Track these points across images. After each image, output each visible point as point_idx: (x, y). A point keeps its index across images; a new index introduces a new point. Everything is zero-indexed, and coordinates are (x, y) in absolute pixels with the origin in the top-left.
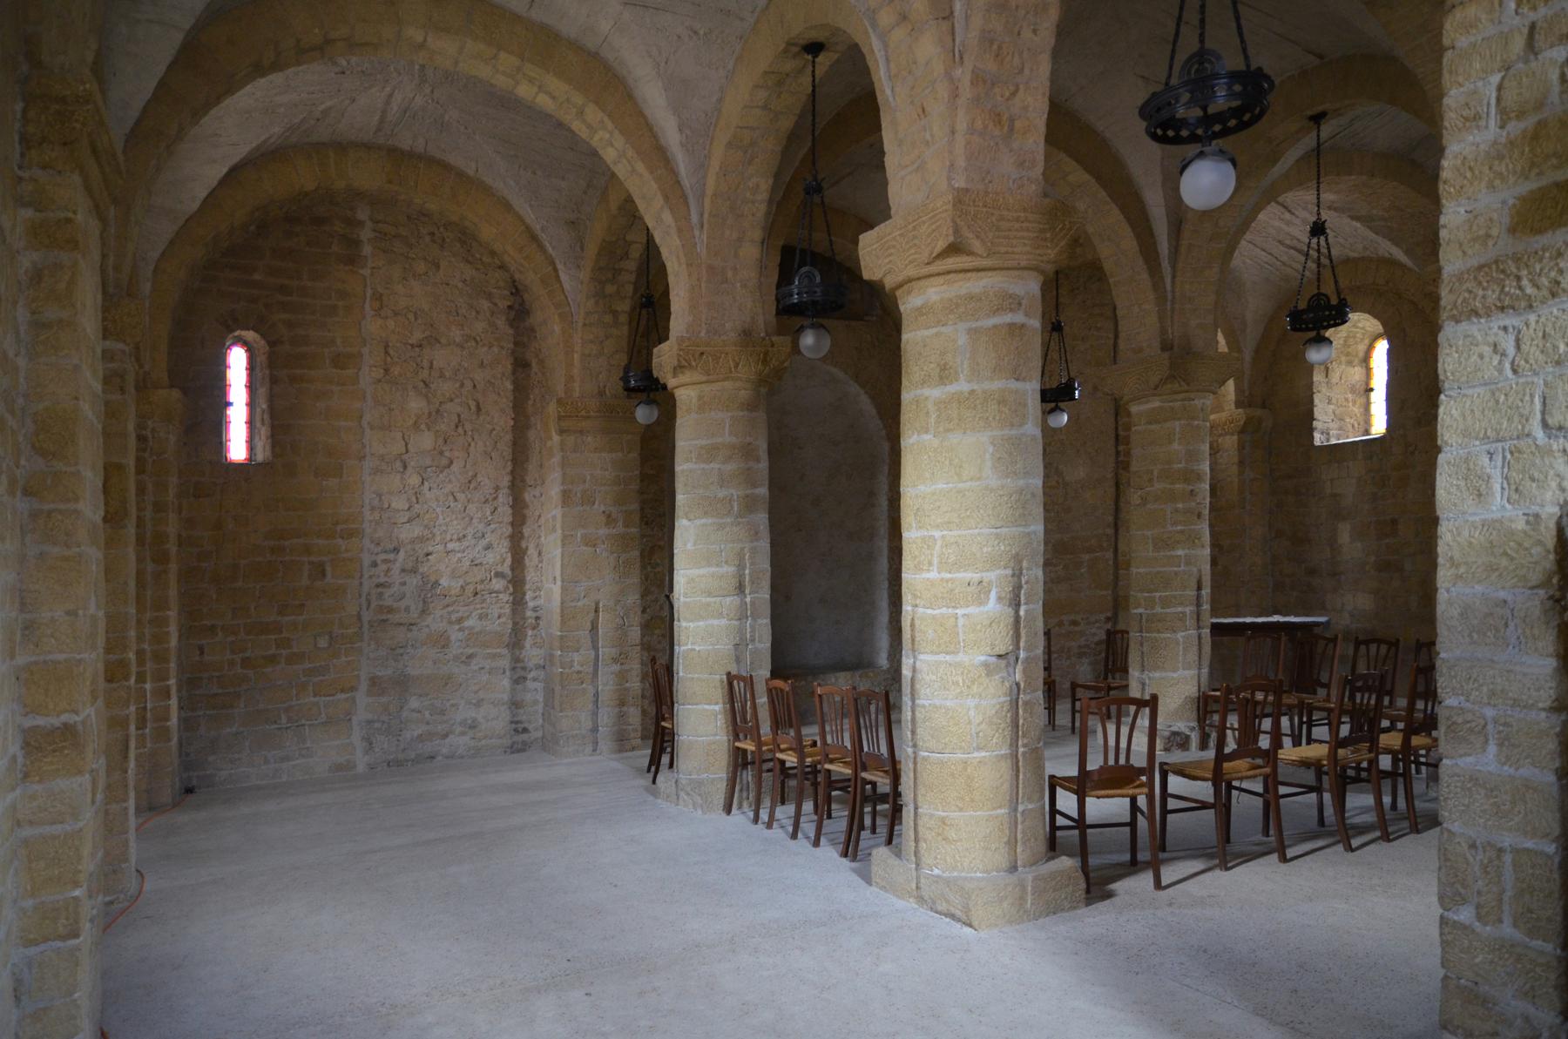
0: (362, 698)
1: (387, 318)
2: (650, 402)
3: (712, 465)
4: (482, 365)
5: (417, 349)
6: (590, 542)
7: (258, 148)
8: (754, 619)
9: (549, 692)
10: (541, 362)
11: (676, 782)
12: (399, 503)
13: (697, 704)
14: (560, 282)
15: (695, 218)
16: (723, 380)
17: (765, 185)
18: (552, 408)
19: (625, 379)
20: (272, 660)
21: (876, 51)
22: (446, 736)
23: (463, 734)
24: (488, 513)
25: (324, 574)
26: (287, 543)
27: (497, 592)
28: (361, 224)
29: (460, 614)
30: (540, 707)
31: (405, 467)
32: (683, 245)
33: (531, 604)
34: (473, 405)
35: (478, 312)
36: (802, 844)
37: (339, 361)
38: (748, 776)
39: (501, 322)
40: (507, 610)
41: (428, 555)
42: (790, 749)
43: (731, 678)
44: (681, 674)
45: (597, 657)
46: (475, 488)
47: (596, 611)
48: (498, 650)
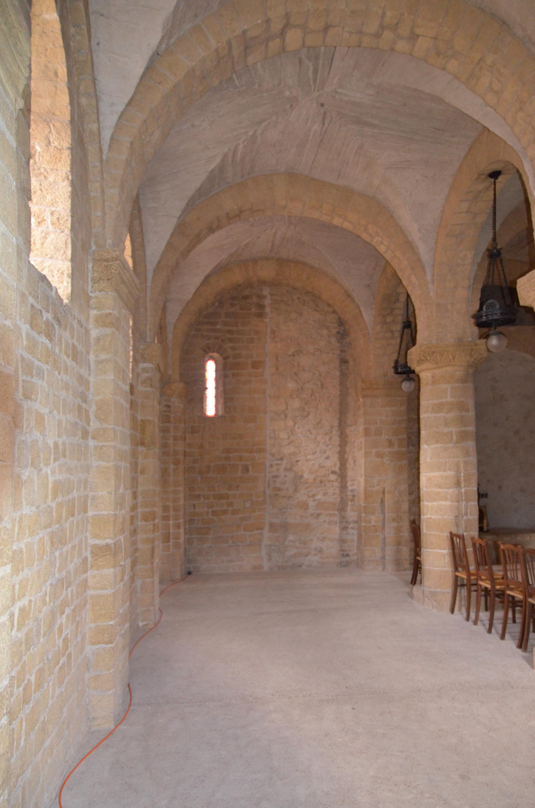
0: (266, 534)
2: (410, 379)
5: (292, 357)
6: (379, 455)
8: (467, 502)
9: (360, 536)
11: (423, 592)
12: (283, 435)
13: (433, 549)
14: (363, 317)
15: (429, 277)
20: (225, 512)
21: (527, 171)
22: (307, 555)
23: (315, 555)
24: (327, 440)
25: (248, 470)
26: (231, 455)
27: (333, 481)
29: (313, 493)
30: (355, 543)
31: (286, 416)
33: (350, 488)
34: (319, 383)
35: (321, 336)
36: (495, 637)
37: (256, 365)
38: (464, 592)
39: (333, 340)
40: (338, 491)
41: (297, 461)
42: (487, 579)
43: (452, 536)
44: (424, 531)
45: (384, 518)
47: (384, 493)
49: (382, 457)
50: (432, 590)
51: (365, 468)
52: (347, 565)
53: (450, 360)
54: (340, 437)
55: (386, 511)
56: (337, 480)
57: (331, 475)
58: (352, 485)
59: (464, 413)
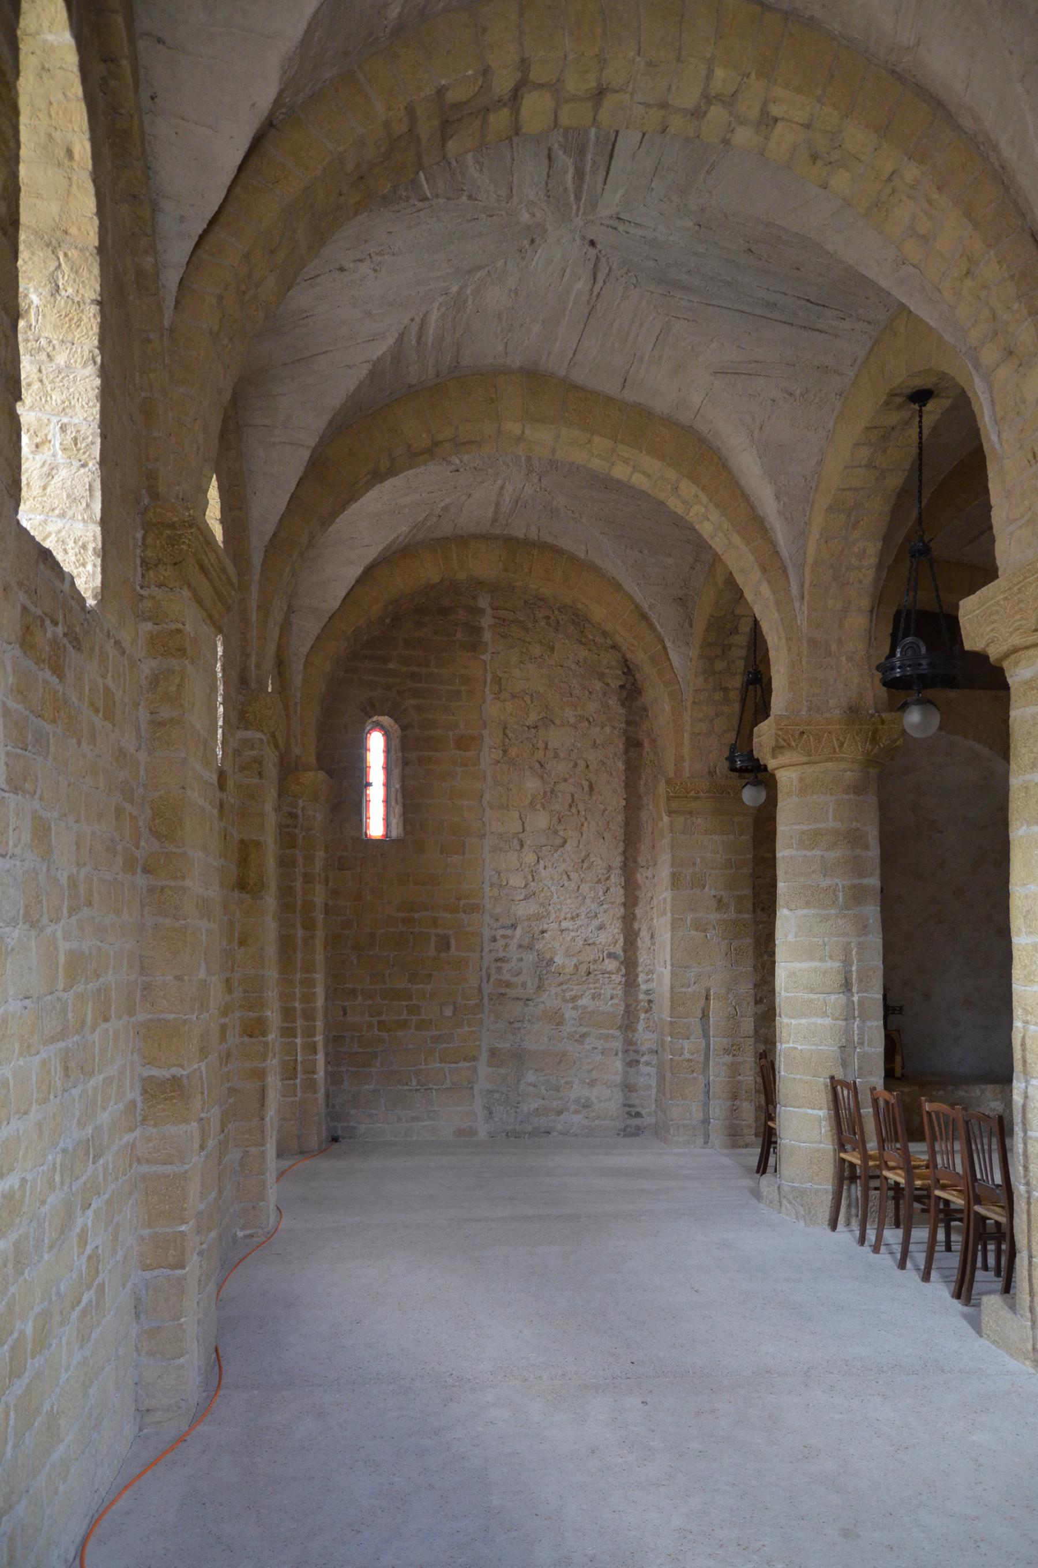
0: (483, 1068)
1: (505, 700)
2: (757, 783)
3: (814, 852)
4: (594, 745)
5: (533, 730)
6: (699, 926)
7: (389, 546)
8: (863, 1020)
9: (661, 1078)
10: (654, 741)
11: (779, 1188)
16: (827, 760)
17: (872, 549)
18: (662, 788)
19: (731, 759)
20: (404, 1025)
21: (980, 394)
22: (560, 1112)
23: (577, 1112)
24: (601, 893)
25: (448, 946)
26: (416, 915)
28: (481, 611)
29: (573, 993)
31: (522, 846)
32: (782, 619)
33: (643, 987)
34: (585, 784)
36: (911, 1276)
37: (464, 743)
38: (857, 1190)
39: (613, 702)
40: (620, 992)
41: (543, 932)
43: (834, 1084)
44: (782, 1073)
46: (588, 868)
47: (707, 998)
48: (611, 1032)
49: (705, 931)
50: (795, 1185)
51: (672, 950)
52: (636, 1132)
53: (834, 748)
54: (624, 888)
55: (711, 1034)
56: (619, 969)
57: (607, 961)
58: (648, 981)
59: (858, 851)
